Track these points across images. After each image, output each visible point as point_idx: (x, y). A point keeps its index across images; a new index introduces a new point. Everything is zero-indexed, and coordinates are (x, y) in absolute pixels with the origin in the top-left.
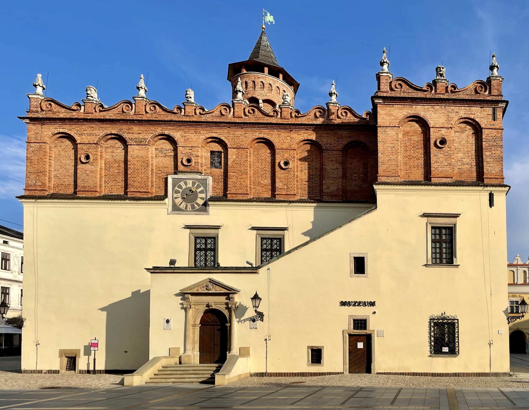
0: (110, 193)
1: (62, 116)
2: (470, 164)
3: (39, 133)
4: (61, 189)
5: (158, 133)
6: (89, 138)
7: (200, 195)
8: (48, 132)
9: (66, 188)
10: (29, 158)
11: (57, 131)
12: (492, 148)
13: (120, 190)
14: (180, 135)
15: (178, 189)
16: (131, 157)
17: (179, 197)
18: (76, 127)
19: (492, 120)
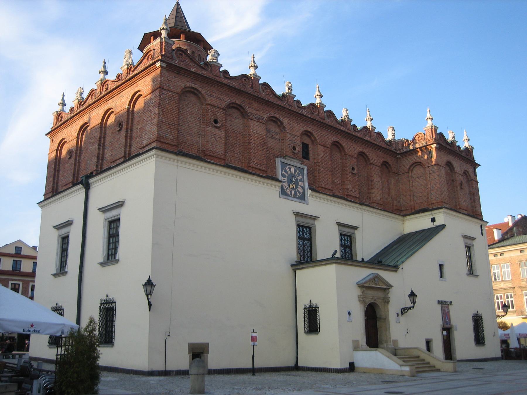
0: (229, 163)
3: (171, 81)
9: (189, 147)
10: (162, 105)
11: (190, 84)
13: (237, 163)
14: (287, 122)
17: (285, 182)
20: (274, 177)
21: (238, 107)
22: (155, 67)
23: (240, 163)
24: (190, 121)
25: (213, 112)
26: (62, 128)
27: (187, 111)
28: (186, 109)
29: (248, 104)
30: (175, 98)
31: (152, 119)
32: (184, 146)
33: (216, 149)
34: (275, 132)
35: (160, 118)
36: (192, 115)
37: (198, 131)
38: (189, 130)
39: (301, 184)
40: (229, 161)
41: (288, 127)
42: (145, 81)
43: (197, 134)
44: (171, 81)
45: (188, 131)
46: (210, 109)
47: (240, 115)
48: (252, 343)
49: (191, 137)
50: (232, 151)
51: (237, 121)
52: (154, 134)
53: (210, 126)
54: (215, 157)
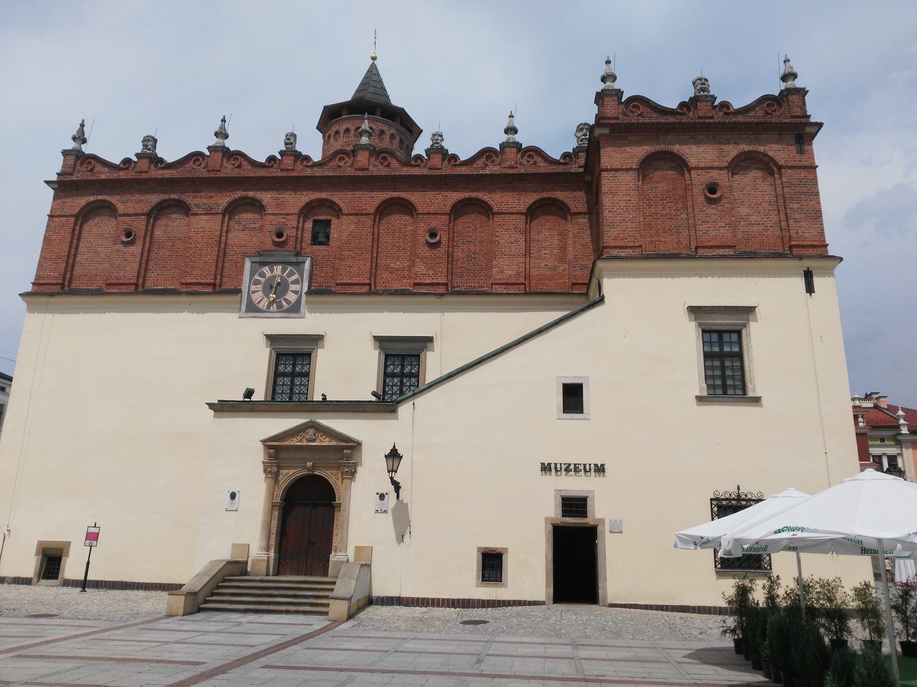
0: (154, 286)
2: (762, 224)
4: (82, 283)
7: (293, 287)
9: (90, 280)
12: (800, 198)
15: (259, 278)
16: (194, 231)
17: (259, 291)
19: (797, 153)
23: (174, 282)
34: (252, 219)
48: (88, 542)
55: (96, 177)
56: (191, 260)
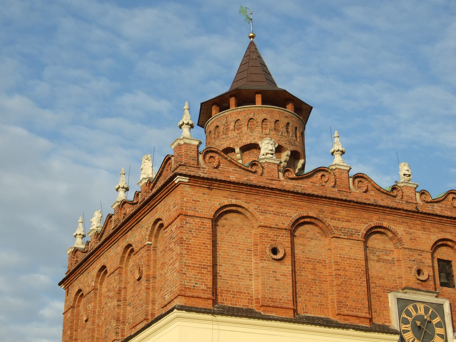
0: (304, 312)
1: (234, 179)
3: (199, 201)
4: (226, 299)
5: (374, 223)
6: (277, 219)
8: (214, 201)
9: (234, 297)
10: (185, 241)
11: (228, 201)
13: (318, 310)
15: (406, 317)
17: (409, 331)
18: (256, 199)
20: (386, 326)
21: (313, 220)
22: (173, 184)
23: (323, 311)
24: (235, 256)
25: (270, 237)
26: (77, 273)
27: (228, 242)
28: (226, 240)
29: (330, 213)
30: (206, 225)
31: (174, 262)
32: (225, 296)
33: (278, 294)
35: (183, 260)
36: (237, 246)
37: (248, 270)
38: (234, 270)
39: (439, 331)
40: (303, 310)
41: (406, 239)
42: (165, 205)
43: (247, 274)
44: (199, 201)
45: (232, 272)
46: (264, 234)
47: (318, 233)
49: (237, 281)
50: (308, 292)
51: (313, 243)
52: (177, 285)
53: (265, 260)
54: (277, 307)
55: (225, 176)
56: (342, 288)
